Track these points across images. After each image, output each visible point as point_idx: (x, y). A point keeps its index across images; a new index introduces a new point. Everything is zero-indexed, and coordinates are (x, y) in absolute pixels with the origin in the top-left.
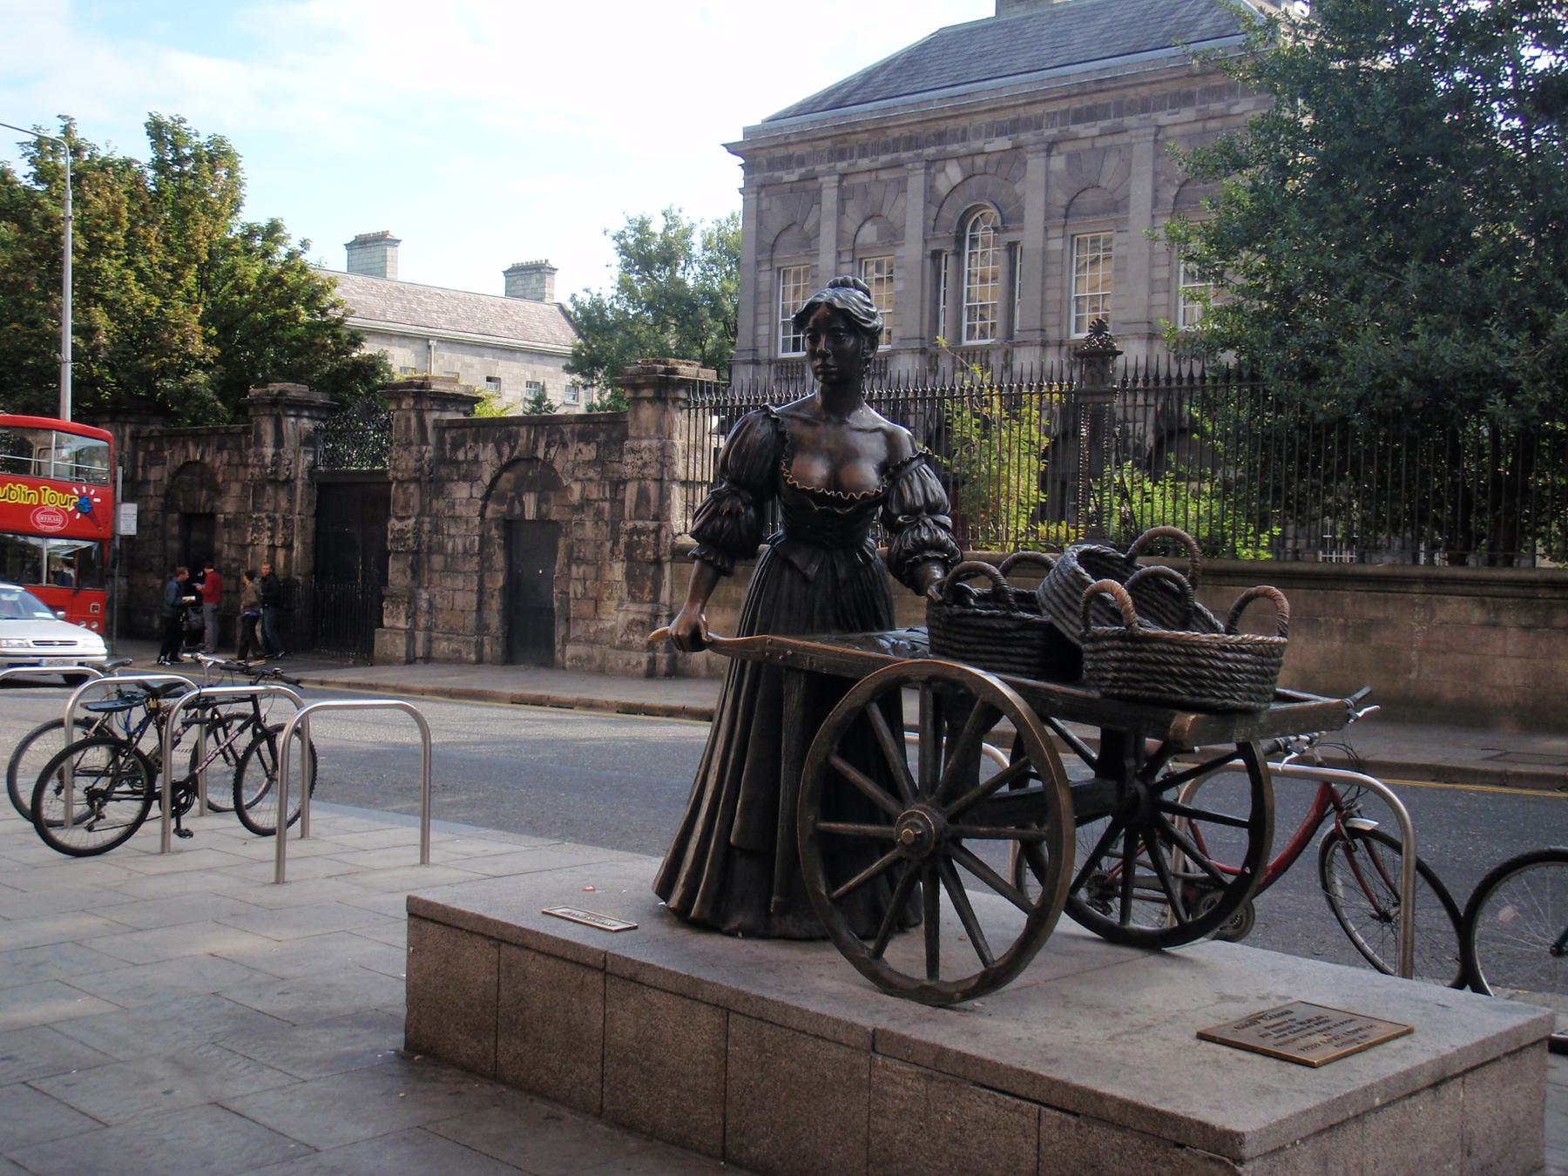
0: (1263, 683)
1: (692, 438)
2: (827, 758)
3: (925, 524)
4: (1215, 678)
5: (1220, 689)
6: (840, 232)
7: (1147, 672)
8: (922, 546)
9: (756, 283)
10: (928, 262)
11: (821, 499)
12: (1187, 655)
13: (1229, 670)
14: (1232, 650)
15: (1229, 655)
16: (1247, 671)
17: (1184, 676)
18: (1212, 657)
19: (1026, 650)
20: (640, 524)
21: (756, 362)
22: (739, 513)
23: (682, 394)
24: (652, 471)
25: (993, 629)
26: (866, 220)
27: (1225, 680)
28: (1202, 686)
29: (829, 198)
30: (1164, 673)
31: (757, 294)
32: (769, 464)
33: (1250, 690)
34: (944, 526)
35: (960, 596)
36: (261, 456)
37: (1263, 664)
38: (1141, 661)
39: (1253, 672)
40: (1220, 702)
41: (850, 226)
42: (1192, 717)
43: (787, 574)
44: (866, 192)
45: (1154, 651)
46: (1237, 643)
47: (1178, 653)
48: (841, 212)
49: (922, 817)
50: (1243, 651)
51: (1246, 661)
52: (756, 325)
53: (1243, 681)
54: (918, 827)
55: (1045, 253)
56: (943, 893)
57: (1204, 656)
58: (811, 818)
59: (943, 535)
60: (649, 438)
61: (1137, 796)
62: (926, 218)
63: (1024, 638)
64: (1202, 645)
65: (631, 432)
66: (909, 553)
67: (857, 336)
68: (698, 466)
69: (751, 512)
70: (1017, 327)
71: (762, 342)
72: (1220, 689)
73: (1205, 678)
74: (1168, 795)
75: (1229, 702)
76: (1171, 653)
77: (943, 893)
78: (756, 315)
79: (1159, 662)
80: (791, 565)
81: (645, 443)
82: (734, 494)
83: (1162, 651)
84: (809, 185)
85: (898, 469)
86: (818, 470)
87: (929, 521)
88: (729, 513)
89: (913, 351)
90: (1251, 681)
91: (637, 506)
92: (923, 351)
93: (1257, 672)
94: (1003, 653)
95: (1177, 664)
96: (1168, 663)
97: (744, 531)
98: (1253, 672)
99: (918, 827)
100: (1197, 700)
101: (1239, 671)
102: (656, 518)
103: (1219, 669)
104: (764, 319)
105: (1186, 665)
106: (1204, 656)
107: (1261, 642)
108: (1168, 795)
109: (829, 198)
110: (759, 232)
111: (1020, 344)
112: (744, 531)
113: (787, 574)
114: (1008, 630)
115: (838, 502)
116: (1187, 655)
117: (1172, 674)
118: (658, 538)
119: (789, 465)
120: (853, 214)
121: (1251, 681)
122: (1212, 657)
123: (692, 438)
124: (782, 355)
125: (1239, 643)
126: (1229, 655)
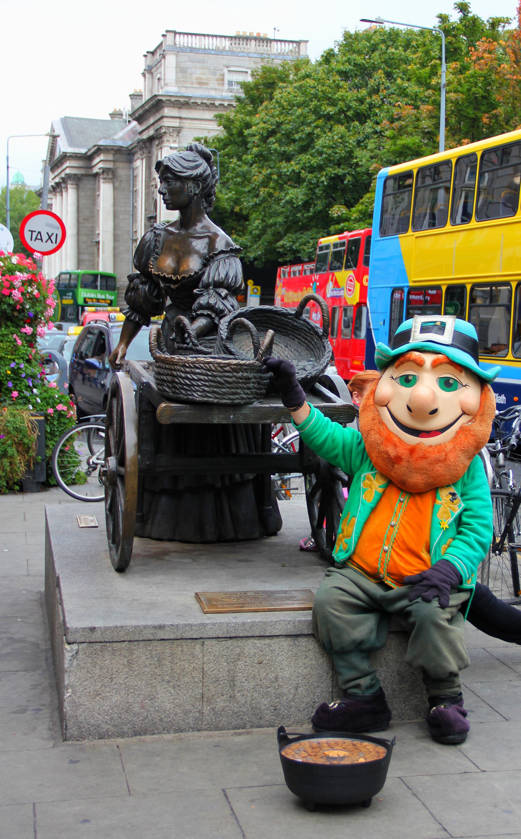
0: (218, 387)
4: (181, 383)
11: (164, 279)
13: (188, 378)
14: (190, 367)
15: (187, 370)
16: (200, 380)
18: (179, 371)
33: (204, 391)
37: (215, 376)
39: (206, 381)
40: (186, 397)
46: (192, 363)
47: (166, 368)
50: (197, 368)
57: (175, 370)
75: (190, 397)
86: (169, 262)
101: (194, 379)
103: (183, 378)
126: (187, 370)
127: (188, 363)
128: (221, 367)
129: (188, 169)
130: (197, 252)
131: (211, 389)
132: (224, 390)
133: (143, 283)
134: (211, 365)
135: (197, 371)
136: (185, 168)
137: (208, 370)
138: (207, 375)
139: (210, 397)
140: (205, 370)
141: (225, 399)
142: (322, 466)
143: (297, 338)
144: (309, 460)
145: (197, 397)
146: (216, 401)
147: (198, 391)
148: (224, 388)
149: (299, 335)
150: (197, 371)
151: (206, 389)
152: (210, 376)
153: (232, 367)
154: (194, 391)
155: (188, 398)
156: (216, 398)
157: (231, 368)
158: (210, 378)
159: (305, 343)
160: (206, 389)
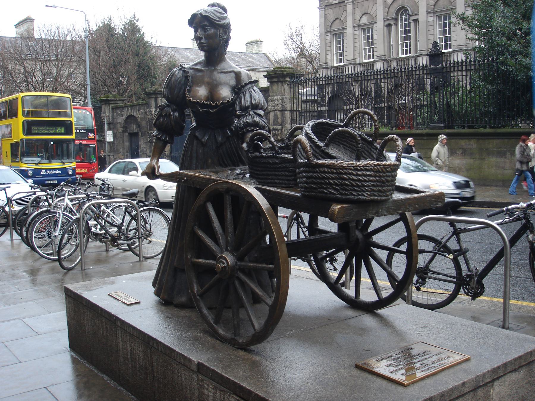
0: (382, 186)
1: (292, 95)
2: (193, 228)
3: (250, 114)
4: (352, 185)
5: (356, 191)
6: (354, 19)
7: (319, 183)
8: (247, 124)
9: (325, 40)
10: (386, 28)
11: (203, 105)
12: (337, 173)
13: (359, 180)
14: (361, 170)
15: (359, 173)
17: (336, 184)
18: (350, 174)
19: (287, 173)
20: (275, 127)
21: (327, 68)
22: (170, 115)
23: (288, 79)
24: (278, 108)
25: (270, 163)
26: (363, 15)
27: (358, 186)
28: (346, 190)
29: (349, 7)
30: (326, 184)
31: (326, 44)
32: (182, 91)
33: (372, 190)
34: (260, 115)
35: (257, 148)
36: (150, 111)
37: (380, 177)
38: (316, 178)
39: (374, 181)
40: (356, 198)
41: (358, 18)
42: (339, 207)
43: (195, 142)
44: (363, 5)
45: (321, 172)
46: (363, 166)
47: (333, 173)
48: (354, 13)
49: (225, 259)
50: (368, 170)
51: (369, 175)
52: (326, 54)
53: (368, 186)
54: (224, 264)
55: (427, 22)
56: (372, 261)
57: (346, 174)
58: (189, 257)
59: (257, 119)
60: (277, 96)
61: (357, 239)
62: (384, 13)
63: (284, 167)
64: (344, 168)
65: (271, 94)
66: (241, 128)
67: (215, 28)
68: (295, 105)
69: (176, 114)
70: (419, 49)
71: (329, 60)
72: (356, 191)
73: (347, 185)
74: (376, 238)
75: (361, 197)
76: (329, 173)
77: (372, 261)
78: (326, 51)
79: (324, 178)
80: (196, 138)
81: (276, 98)
82: (168, 106)
83: (324, 172)
84: (342, 4)
85: (240, 89)
86: (202, 92)
87: (252, 113)
88: (166, 115)
89: (382, 60)
90: (373, 186)
91: (274, 121)
92: (385, 60)
93: (377, 181)
94: (276, 175)
95: (333, 179)
96: (328, 178)
97: (173, 123)
98: (374, 181)
99: (224, 264)
100: (344, 197)
102: (281, 125)
103: (354, 180)
104: (329, 52)
105: (336, 179)
106: (346, 174)
107: (378, 165)
108: (376, 238)
109: (349, 7)
110: (325, 22)
111: (419, 56)
112: (173, 123)
113: (195, 142)
114: (276, 163)
115: (210, 106)
116: (337, 173)
117: (330, 184)
118: (282, 132)
119: (189, 91)
120: (358, 13)
121: (373, 186)
122: (350, 174)
123: (292, 95)
124: (336, 65)
125: (365, 165)
126: (359, 173)
127: (360, 167)
128: (384, 168)
129: (222, 19)
130: (226, 84)
131: (377, 188)
132: (384, 188)
133: (174, 111)
134: (378, 167)
135: (368, 173)
136: (219, 17)
137: (376, 172)
138: (375, 176)
139: (375, 196)
140: (374, 171)
141: (384, 196)
142: (360, 240)
143: (343, 144)
144: (353, 237)
145: (366, 196)
146: (379, 198)
147: (367, 191)
148: (385, 186)
149: (345, 142)
150: (368, 173)
151: (374, 189)
152: (378, 177)
153: (392, 167)
154: (364, 192)
155: (359, 198)
156: (380, 196)
157: (391, 169)
158: (377, 178)
159: (350, 148)
160: (374, 189)
